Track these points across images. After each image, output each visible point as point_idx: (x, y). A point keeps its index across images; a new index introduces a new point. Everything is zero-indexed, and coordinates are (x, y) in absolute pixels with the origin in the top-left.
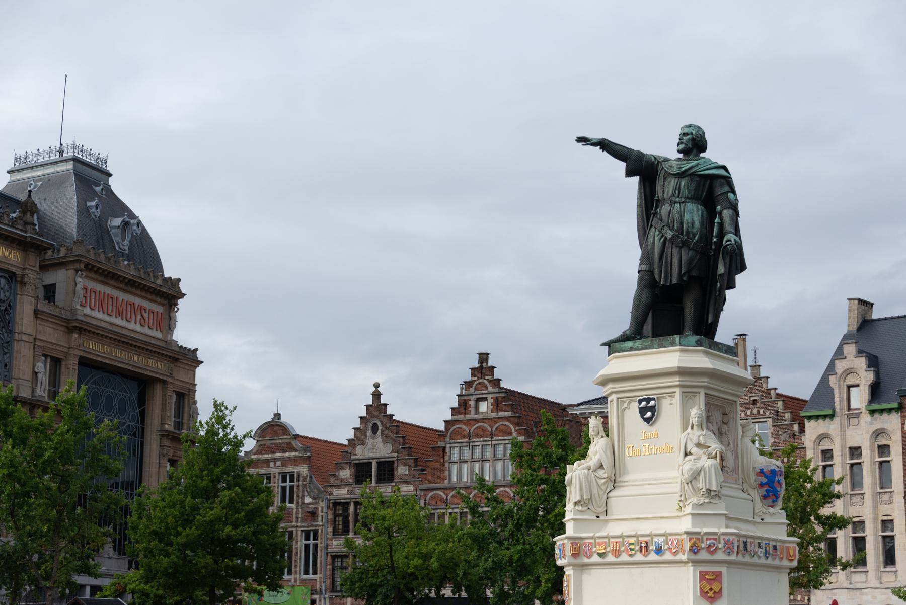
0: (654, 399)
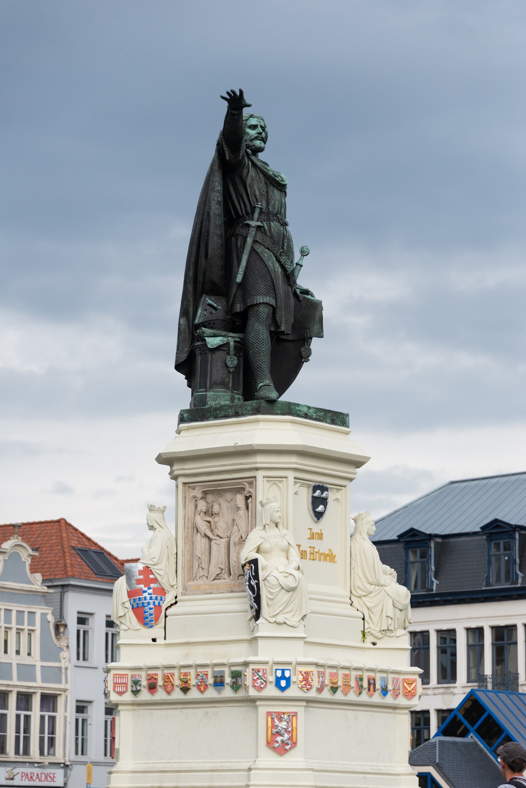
0: (326, 489)
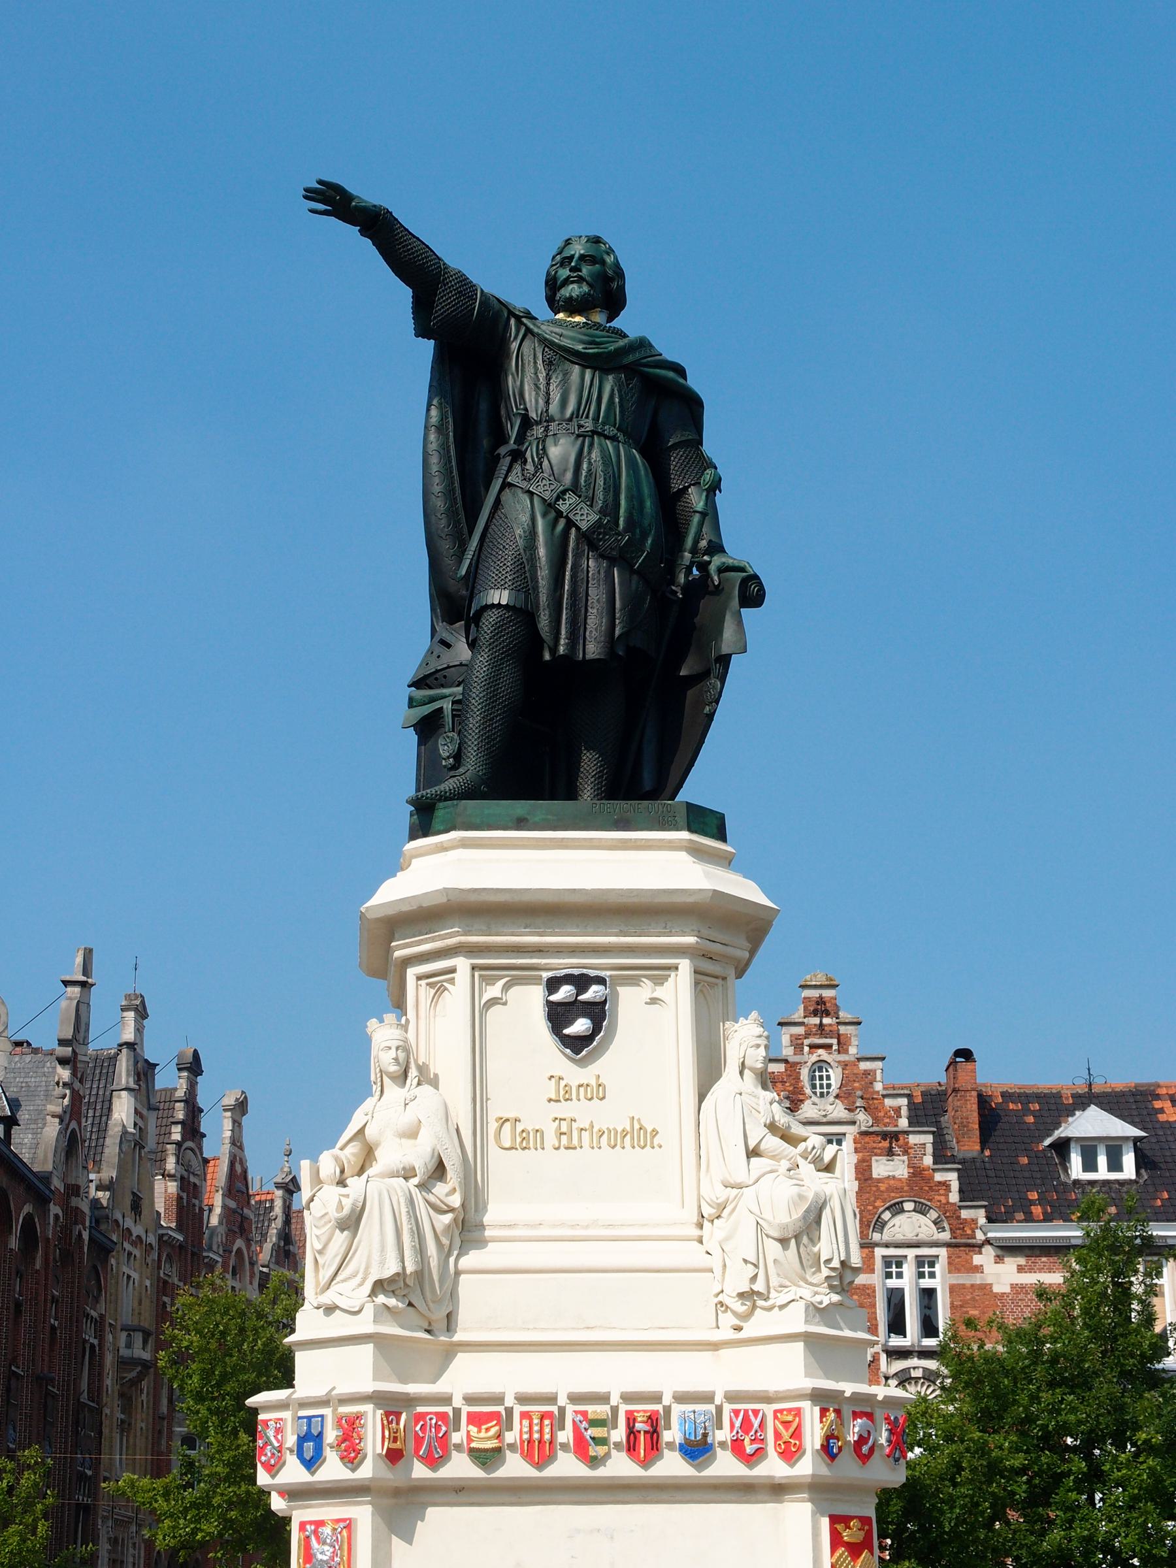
0: (601, 981)
